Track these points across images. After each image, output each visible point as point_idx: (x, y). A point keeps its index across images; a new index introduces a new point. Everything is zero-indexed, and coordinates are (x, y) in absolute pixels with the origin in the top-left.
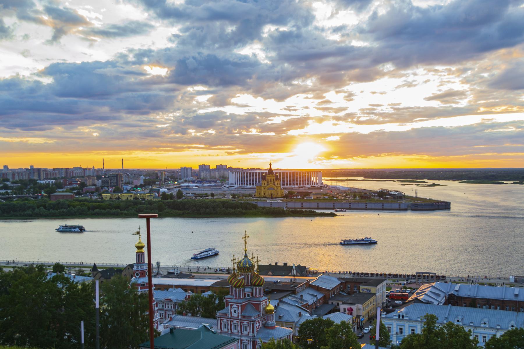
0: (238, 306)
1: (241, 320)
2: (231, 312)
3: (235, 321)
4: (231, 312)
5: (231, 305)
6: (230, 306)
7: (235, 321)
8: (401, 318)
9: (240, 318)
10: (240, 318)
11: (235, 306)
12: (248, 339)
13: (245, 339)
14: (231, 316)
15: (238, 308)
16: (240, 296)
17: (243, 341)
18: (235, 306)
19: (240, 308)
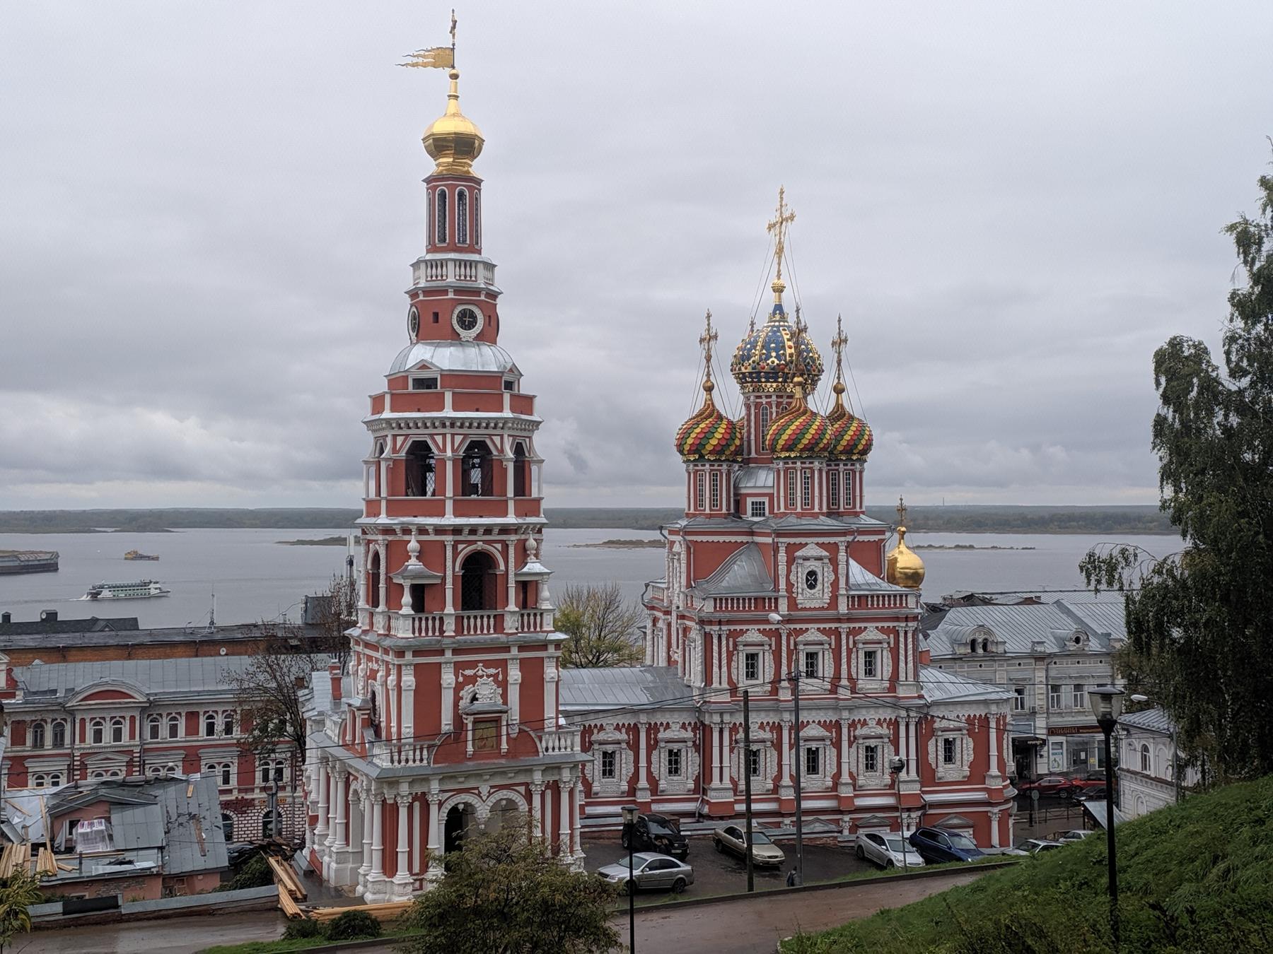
0: (833, 549)
1: (849, 620)
2: (790, 585)
3: (813, 634)
4: (790, 585)
5: (791, 549)
6: (782, 557)
7: (813, 633)
8: (980, 651)
9: (843, 608)
10: (843, 608)
11: (812, 550)
12: (888, 714)
13: (871, 716)
14: (793, 604)
15: (834, 562)
16: (808, 500)
17: (860, 731)
18: (812, 550)
19: (842, 556)
